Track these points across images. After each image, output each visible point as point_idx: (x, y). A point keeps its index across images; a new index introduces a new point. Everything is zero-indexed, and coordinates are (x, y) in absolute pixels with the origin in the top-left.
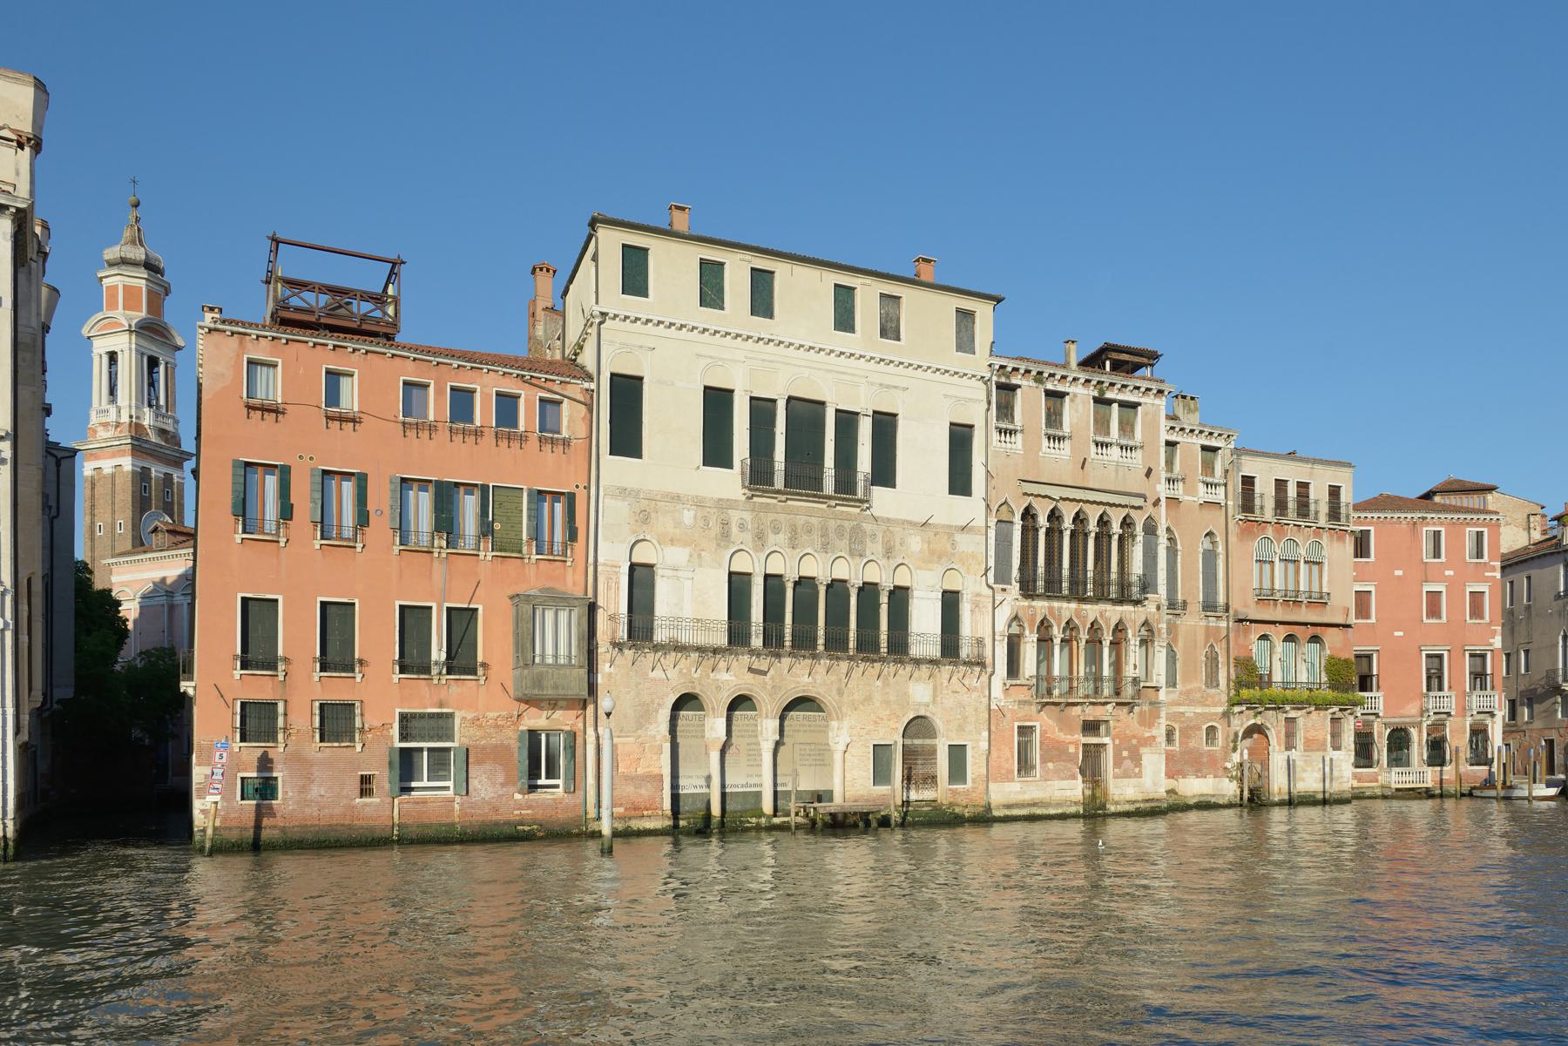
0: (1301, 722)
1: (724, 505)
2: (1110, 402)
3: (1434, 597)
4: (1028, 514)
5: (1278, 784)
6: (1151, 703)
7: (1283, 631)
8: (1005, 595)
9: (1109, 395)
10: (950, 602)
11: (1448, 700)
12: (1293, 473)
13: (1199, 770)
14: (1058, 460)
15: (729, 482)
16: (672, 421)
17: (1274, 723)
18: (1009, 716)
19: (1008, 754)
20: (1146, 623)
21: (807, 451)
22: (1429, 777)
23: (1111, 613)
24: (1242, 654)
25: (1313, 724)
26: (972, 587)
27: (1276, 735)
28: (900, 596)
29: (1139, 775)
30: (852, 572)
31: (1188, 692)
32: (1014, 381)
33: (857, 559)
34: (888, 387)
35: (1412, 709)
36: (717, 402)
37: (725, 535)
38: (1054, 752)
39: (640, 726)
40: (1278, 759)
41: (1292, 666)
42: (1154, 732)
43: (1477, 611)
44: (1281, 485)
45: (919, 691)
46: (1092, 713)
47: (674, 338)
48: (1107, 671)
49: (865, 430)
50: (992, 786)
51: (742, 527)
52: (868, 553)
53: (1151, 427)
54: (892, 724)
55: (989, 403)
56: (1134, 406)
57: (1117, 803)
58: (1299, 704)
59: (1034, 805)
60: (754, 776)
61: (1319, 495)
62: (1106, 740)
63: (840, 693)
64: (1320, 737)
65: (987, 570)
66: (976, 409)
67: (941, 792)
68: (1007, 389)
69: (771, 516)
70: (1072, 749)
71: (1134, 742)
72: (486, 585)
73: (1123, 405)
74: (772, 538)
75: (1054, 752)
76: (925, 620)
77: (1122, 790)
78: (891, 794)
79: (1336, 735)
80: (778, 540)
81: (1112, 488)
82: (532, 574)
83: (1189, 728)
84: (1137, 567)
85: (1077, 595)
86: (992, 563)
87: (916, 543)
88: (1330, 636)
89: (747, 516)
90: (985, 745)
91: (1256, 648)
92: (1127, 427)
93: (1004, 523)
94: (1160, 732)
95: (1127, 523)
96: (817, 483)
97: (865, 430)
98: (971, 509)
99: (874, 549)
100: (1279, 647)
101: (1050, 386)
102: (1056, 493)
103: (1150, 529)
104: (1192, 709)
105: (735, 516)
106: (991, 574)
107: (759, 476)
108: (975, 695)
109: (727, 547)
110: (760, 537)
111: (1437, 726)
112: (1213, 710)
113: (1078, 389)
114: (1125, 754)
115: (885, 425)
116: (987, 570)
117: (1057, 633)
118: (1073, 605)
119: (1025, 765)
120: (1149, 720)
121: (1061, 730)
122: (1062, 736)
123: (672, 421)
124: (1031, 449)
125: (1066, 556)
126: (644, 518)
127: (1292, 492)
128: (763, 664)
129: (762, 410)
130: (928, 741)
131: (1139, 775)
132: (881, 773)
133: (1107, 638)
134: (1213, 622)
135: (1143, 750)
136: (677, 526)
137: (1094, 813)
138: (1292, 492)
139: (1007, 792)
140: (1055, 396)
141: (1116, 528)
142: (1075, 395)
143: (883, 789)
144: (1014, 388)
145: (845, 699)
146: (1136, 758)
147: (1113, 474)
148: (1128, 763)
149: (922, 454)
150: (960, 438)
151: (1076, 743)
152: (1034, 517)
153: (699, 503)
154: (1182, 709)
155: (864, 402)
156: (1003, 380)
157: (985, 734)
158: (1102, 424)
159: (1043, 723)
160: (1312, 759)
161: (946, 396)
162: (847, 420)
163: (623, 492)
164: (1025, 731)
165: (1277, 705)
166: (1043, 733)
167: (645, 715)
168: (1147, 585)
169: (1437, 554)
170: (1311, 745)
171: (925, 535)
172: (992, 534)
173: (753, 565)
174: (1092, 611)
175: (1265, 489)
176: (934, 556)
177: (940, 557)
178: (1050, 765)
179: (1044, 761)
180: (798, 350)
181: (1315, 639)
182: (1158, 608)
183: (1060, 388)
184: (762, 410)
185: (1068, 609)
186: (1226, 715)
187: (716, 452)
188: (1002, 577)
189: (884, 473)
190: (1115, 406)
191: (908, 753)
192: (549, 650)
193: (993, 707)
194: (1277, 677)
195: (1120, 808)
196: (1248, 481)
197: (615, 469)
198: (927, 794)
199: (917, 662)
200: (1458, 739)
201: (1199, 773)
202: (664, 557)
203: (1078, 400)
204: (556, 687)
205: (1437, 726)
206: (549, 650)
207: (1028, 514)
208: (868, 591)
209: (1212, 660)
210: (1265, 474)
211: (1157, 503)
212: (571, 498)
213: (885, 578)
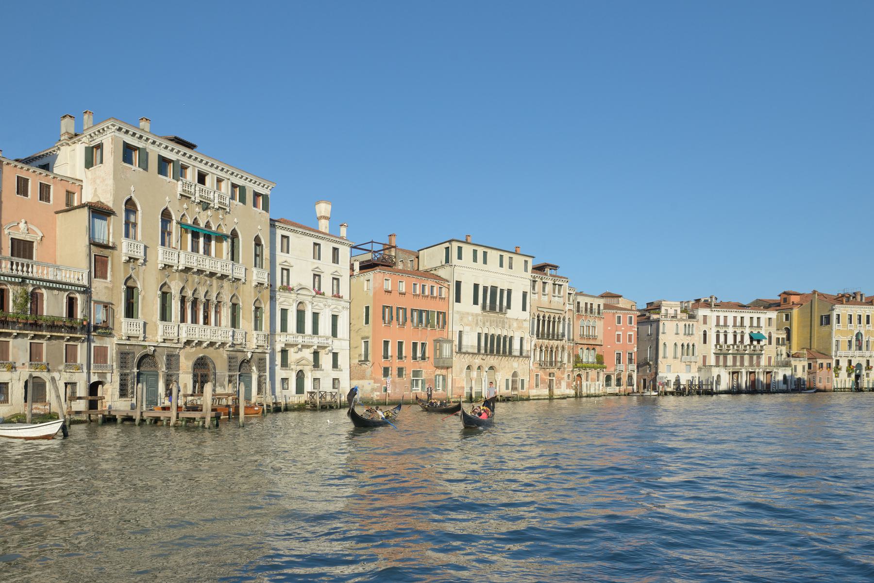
1: (477, 315)
3: (619, 335)
4: (538, 317)
5: (585, 391)
7: (586, 347)
10: (522, 339)
11: (622, 367)
12: (589, 300)
15: (478, 309)
16: (467, 293)
17: (583, 373)
21: (493, 300)
22: (617, 390)
23: (555, 343)
25: (593, 373)
27: (584, 377)
28: (511, 338)
35: (612, 369)
38: (543, 381)
40: (584, 383)
41: (588, 357)
43: (630, 340)
44: (586, 304)
46: (552, 371)
47: (470, 272)
53: (565, 291)
58: (590, 368)
61: (595, 307)
67: (519, 392)
68: (534, 281)
72: (427, 336)
76: (516, 345)
77: (557, 392)
78: (509, 392)
79: (598, 377)
82: (438, 334)
84: (561, 331)
85: (548, 338)
88: (597, 348)
91: (580, 351)
94: (566, 376)
95: (559, 318)
96: (495, 309)
98: (526, 315)
100: (585, 351)
103: (564, 320)
105: (479, 318)
107: (484, 308)
111: (619, 374)
115: (509, 292)
117: (543, 348)
120: (563, 373)
123: (467, 293)
124: (539, 298)
125: (546, 328)
127: (589, 306)
128: (484, 357)
129: (485, 289)
132: (507, 388)
136: (467, 322)
137: (551, 398)
138: (589, 306)
139: (533, 392)
140: (544, 283)
141: (557, 319)
146: (560, 383)
150: (525, 295)
153: (472, 315)
155: (505, 288)
159: (541, 373)
160: (594, 385)
162: (502, 291)
164: (537, 375)
165: (585, 368)
167: (461, 371)
168: (563, 335)
169: (619, 323)
170: (592, 380)
171: (517, 324)
174: (551, 342)
175: (582, 305)
180: (492, 274)
181: (594, 349)
184: (485, 289)
186: (572, 371)
188: (533, 334)
189: (509, 306)
191: (513, 381)
194: (584, 360)
196: (579, 303)
198: (516, 393)
199: (515, 357)
200: (624, 379)
205: (619, 374)
210: (582, 300)
212: (444, 313)
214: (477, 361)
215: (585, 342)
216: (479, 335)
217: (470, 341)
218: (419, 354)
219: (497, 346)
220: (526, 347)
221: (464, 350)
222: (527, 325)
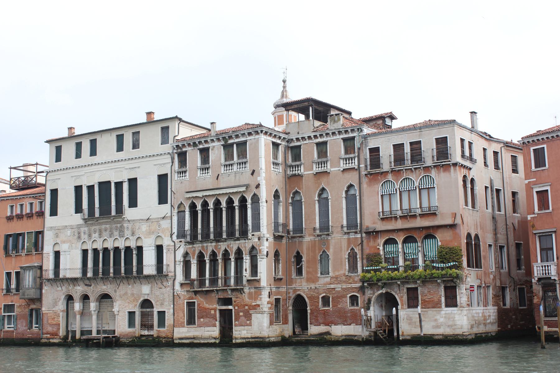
0: (420, 289)
1: (79, 227)
2: (232, 145)
4: (193, 207)
6: (255, 288)
8: (181, 243)
9: (230, 141)
13: (346, 321)
14: (205, 180)
16: (66, 200)
18: (182, 298)
19: (182, 315)
20: (253, 248)
24: (373, 251)
26: (166, 242)
29: (250, 325)
30: (121, 244)
31: (336, 278)
32: (184, 149)
33: (122, 238)
34: (132, 168)
36: (78, 189)
37: (79, 237)
39: (54, 307)
42: (258, 303)
45: (145, 290)
48: (220, 273)
49: (126, 187)
50: (176, 330)
51: (85, 233)
52: (126, 235)
54: (135, 303)
55: (173, 162)
56: (245, 143)
57: (236, 339)
59: (194, 338)
60: (93, 325)
62: (230, 307)
63: (115, 291)
64: (436, 299)
65: (171, 235)
66: (166, 165)
69: (93, 227)
70: (213, 312)
71: (247, 307)
73: (238, 144)
74: (94, 235)
75: (205, 313)
76: (149, 258)
78: (137, 330)
80: (95, 236)
81: (233, 185)
83: (338, 297)
86: (175, 230)
87: (144, 227)
89: (86, 229)
90: (172, 311)
92: (243, 154)
93: (181, 213)
97: (126, 187)
98: (165, 209)
99: (127, 233)
101: (201, 147)
102: (200, 194)
104: (339, 286)
105: (82, 230)
106: (174, 237)
108: (168, 289)
109: (80, 241)
110: (90, 236)
112: (354, 285)
113: (216, 144)
114: (241, 314)
115: (133, 182)
116: (171, 235)
118: (214, 244)
119: (191, 321)
121: (207, 303)
122: (207, 306)
123: (66, 200)
126: (57, 236)
129: (91, 188)
130: (152, 310)
131: (250, 325)
132: (131, 323)
133: (232, 257)
134: (352, 236)
135: (251, 312)
139: (182, 332)
142: (214, 147)
143: (131, 330)
144: (185, 153)
145: (118, 293)
146: (248, 317)
147: (233, 178)
148: (243, 319)
149: (148, 191)
151: (215, 310)
152: (196, 207)
153: (72, 228)
154: (332, 286)
155: (124, 177)
156: (179, 150)
157: (172, 306)
158: (229, 156)
159: (198, 300)
161: (155, 165)
162: (119, 185)
163: (51, 228)
166: (199, 305)
167: (55, 303)
171: (151, 224)
172: (175, 219)
173: (89, 246)
176: (150, 233)
177: (153, 232)
178: (202, 320)
179: (199, 318)
182: (259, 239)
183: (206, 146)
185: (210, 247)
187: (78, 209)
190: (235, 146)
192: (27, 284)
193: (175, 294)
195: (239, 341)
197: (49, 221)
201: (345, 322)
202: (63, 248)
203: (215, 149)
204: (28, 295)
206: (27, 284)
207: (193, 207)
208: (128, 249)
209: (352, 257)
211: (258, 186)
213: (132, 244)
214: (78, 290)
215: (399, 224)
216: (85, 252)
217: (71, 265)
218: (13, 286)
219: (116, 265)
220: (167, 258)
221: (61, 276)
222: (165, 224)
